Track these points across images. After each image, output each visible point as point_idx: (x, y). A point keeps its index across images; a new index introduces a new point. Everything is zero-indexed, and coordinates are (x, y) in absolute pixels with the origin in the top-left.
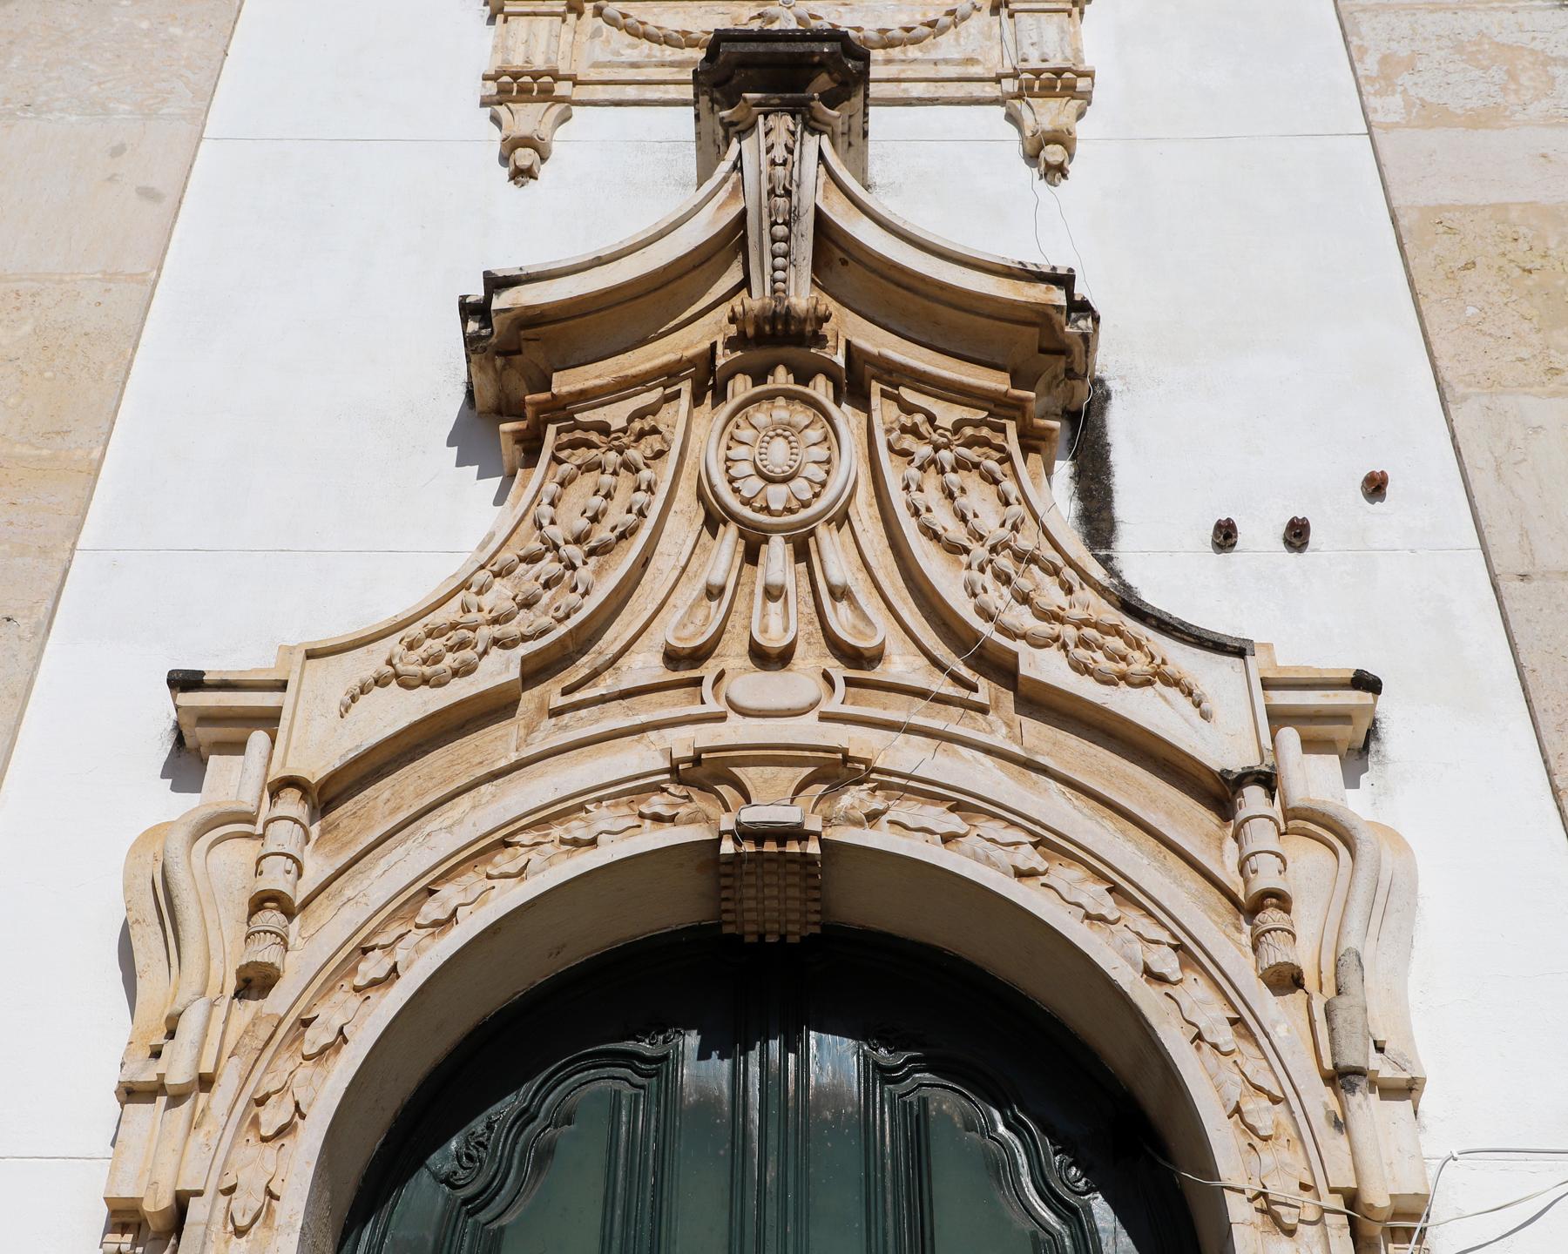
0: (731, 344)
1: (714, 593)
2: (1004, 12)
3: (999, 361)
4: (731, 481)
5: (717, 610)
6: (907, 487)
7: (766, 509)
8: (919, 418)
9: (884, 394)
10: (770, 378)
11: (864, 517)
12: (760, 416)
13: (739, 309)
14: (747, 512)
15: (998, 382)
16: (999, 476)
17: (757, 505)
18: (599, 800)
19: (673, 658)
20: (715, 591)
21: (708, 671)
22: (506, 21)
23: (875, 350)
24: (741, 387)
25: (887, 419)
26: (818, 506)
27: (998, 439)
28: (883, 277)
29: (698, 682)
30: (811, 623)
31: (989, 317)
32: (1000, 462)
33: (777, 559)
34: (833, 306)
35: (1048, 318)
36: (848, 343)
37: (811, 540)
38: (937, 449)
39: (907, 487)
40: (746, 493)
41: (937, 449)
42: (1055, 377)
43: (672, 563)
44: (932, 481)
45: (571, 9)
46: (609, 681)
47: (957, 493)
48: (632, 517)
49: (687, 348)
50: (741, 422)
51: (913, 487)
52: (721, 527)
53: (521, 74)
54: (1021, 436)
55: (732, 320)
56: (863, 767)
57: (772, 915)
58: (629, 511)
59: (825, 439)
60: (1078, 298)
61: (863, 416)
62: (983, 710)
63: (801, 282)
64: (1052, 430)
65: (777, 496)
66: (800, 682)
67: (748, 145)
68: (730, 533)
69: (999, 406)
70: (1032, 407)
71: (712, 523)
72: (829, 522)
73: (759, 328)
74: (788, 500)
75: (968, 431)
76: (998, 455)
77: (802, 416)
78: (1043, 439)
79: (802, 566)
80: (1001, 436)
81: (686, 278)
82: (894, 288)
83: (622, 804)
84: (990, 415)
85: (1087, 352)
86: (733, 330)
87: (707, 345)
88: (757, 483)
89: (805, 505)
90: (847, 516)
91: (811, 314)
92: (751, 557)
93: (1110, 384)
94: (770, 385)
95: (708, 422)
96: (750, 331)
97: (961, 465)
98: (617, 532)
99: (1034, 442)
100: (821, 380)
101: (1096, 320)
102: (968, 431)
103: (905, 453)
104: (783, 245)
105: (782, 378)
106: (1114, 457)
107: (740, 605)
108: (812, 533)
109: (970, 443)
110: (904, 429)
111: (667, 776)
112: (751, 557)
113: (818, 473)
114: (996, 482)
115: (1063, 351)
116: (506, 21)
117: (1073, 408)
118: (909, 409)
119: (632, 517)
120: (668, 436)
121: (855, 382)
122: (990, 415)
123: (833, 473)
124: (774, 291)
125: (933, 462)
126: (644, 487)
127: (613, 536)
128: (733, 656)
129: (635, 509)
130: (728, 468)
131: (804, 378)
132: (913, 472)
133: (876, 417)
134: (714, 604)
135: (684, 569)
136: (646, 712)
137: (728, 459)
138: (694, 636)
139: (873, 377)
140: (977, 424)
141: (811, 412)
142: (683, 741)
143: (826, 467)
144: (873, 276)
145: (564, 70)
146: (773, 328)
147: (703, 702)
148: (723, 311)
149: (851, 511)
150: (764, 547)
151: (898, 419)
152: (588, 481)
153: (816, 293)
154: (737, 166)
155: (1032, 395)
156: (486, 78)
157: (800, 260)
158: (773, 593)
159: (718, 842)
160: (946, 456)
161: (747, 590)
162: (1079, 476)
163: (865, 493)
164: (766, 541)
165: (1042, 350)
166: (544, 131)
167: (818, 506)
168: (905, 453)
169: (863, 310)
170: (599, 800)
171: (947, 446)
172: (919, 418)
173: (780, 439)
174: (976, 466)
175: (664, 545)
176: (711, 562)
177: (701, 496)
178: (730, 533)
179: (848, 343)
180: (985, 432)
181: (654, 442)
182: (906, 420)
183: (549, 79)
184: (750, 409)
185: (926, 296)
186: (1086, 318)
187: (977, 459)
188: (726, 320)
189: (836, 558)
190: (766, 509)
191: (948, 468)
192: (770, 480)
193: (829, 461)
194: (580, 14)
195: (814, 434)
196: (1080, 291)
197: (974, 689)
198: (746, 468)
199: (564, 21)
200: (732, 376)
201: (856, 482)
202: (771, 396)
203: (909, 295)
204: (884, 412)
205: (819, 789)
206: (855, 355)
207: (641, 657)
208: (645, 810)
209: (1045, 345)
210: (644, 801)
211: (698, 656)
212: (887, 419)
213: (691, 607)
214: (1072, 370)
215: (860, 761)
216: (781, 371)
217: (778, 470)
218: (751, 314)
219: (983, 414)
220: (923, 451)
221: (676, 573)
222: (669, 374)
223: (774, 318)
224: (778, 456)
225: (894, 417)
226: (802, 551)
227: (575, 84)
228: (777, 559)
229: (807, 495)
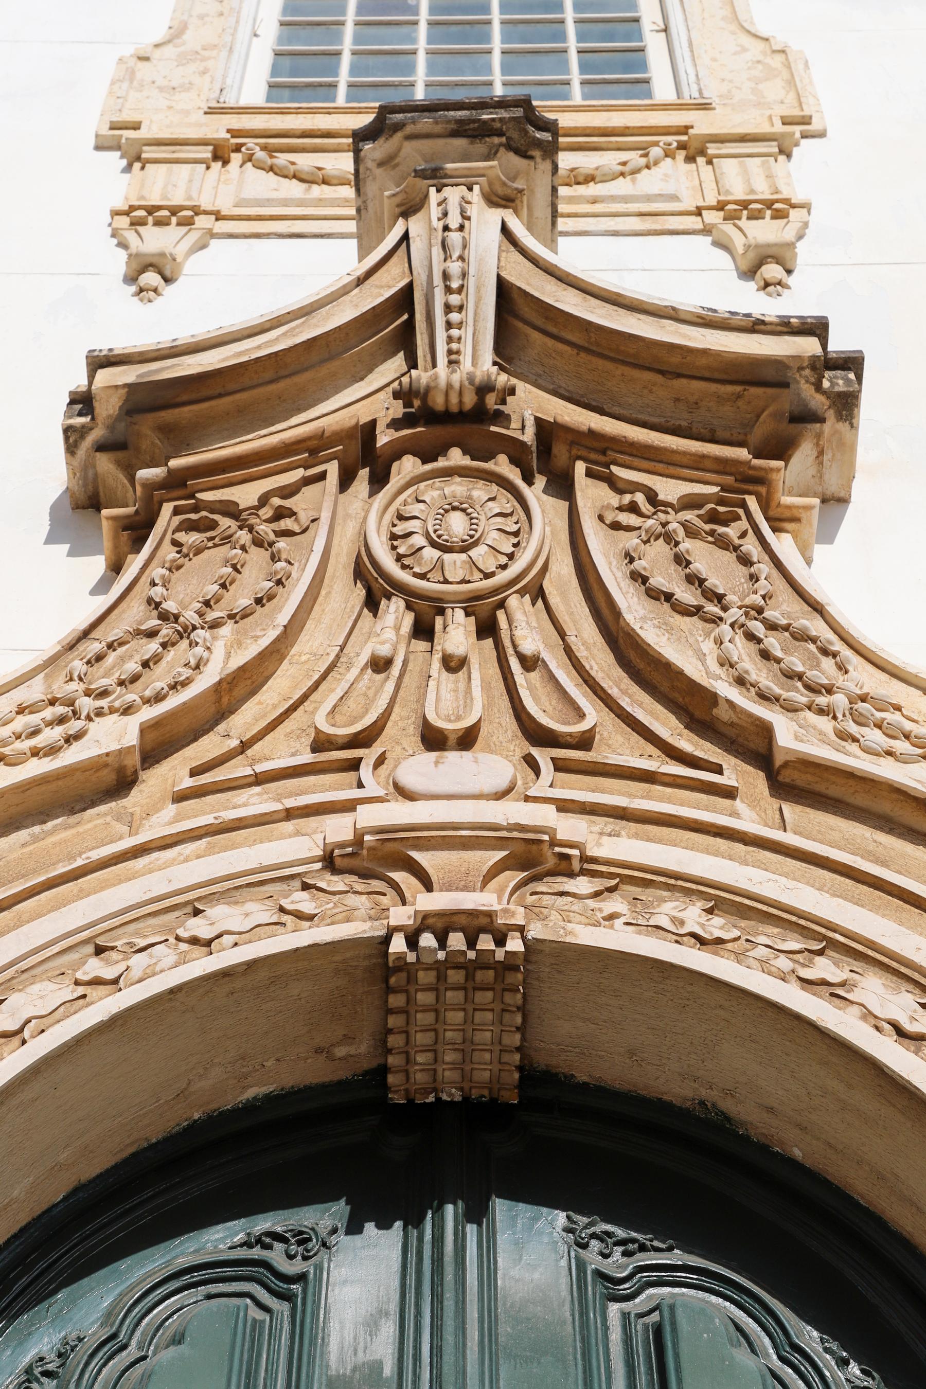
0: (395, 424)
2: (701, 160)
4: (399, 558)
21: (369, 755)
22: (143, 168)
29: (354, 765)
33: (457, 633)
45: (216, 157)
53: (159, 208)
56: (575, 852)
57: (452, 1057)
62: (729, 793)
66: (492, 765)
67: (416, 226)
72: (522, 592)
79: (490, 642)
88: (430, 554)
92: (423, 630)
108: (501, 605)
111: (319, 865)
112: (423, 630)
116: (143, 168)
121: (551, 458)
128: (401, 735)
142: (339, 829)
145: (206, 205)
147: (360, 785)
149: (546, 584)
152: (224, 551)
154: (406, 237)
156: (116, 213)
158: (454, 665)
159: (386, 940)
163: (563, 568)
166: (180, 251)
177: (359, 573)
183: (190, 213)
194: (226, 162)
197: (719, 770)
199: (208, 168)
200: (398, 457)
205: (513, 877)
208: (287, 904)
215: (572, 846)
226: (487, 629)
227: (217, 219)
228: (457, 633)
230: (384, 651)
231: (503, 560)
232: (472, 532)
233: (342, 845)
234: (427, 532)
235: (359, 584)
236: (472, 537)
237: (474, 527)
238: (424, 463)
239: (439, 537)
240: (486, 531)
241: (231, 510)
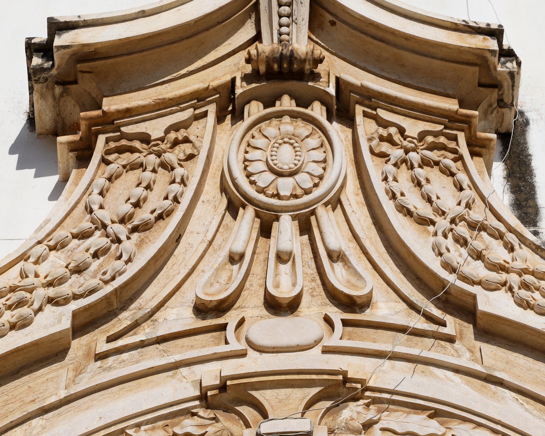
1: (235, 259)
3: (450, 92)
4: (249, 175)
5: (237, 272)
6: (386, 179)
7: (277, 196)
8: (393, 130)
9: (365, 114)
10: (278, 103)
11: (353, 203)
12: (271, 129)
13: (253, 52)
14: (261, 197)
15: (451, 105)
16: (454, 170)
17: (270, 192)
18: (138, 426)
19: (201, 309)
20: (236, 258)
23: (358, 82)
24: (255, 110)
25: (368, 132)
26: (317, 193)
27: (452, 145)
28: (362, 32)
30: (313, 280)
31: (442, 59)
32: (455, 160)
34: (325, 53)
35: (485, 60)
36: (338, 80)
37: (313, 218)
38: (407, 152)
39: (386, 179)
40: (261, 184)
41: (407, 152)
42: (490, 105)
43: (200, 237)
44: (404, 174)
46: (147, 331)
47: (423, 182)
48: (168, 202)
49: (212, 81)
50: (256, 134)
51: (390, 178)
52: (241, 210)
54: (469, 145)
55: (248, 61)
58: (166, 198)
59: (322, 145)
60: (505, 47)
61: (349, 131)
63: (301, 36)
64: (491, 140)
65: (285, 186)
68: (248, 215)
69: (451, 120)
70: (476, 121)
71: (233, 209)
72: (326, 205)
73: (269, 66)
74: (294, 189)
75: (430, 139)
76: (453, 156)
77: (303, 129)
78: (484, 146)
79: (306, 237)
80: (455, 143)
81: (212, 31)
82: (371, 40)
83: (159, 428)
84: (446, 128)
85: (513, 86)
86: (249, 69)
87: (228, 78)
88: (270, 177)
89: (307, 192)
90: (339, 201)
91: (309, 57)
93: (528, 115)
94: (278, 107)
95: (230, 135)
96: (262, 69)
97: (425, 163)
98: (156, 214)
99: (477, 149)
100: (317, 105)
101: (519, 64)
102: (430, 139)
103: (383, 155)
104: (287, 8)
105: (287, 103)
106: (535, 164)
107: (257, 269)
108: (313, 213)
109: (432, 147)
110: (382, 139)
111: (197, 403)
113: (317, 170)
114: (452, 175)
115: (495, 85)
117: (503, 130)
118: (385, 124)
119: (168, 202)
120: (197, 144)
122: (446, 128)
123: (328, 170)
124: (280, 41)
125: (404, 161)
126: (178, 180)
127: (153, 217)
129: (171, 197)
130: (245, 168)
131: (304, 102)
132: (390, 167)
133: (360, 130)
134: (236, 267)
135: (211, 243)
136: (180, 353)
137: (246, 160)
138: (220, 292)
139: (358, 103)
140: (436, 134)
141: (310, 127)
142: (210, 374)
143: (323, 165)
144: (355, 32)
146: (280, 66)
148: (243, 55)
149: (343, 198)
150: (275, 224)
151: (377, 131)
153: (312, 45)
155: (476, 113)
157: (300, 20)
158: (282, 258)
160: (414, 157)
161: (262, 257)
162: (510, 176)
164: (277, 219)
165: (481, 85)
167: (317, 193)
168: (383, 155)
169: (348, 57)
170: (138, 426)
171: (414, 150)
172: (393, 130)
173: (287, 145)
174: (437, 163)
175: (193, 225)
176: (233, 236)
177: (224, 189)
178: (248, 215)
179: (338, 79)
180: (442, 140)
181: (187, 149)
182: (384, 132)
184: (263, 125)
185: (395, 46)
186: (512, 61)
187: (437, 159)
188: (243, 62)
189: (332, 231)
190: (277, 196)
191: (416, 165)
192: (280, 174)
193: (325, 161)
195: (314, 142)
196: (507, 43)
198: (262, 166)
200: (249, 102)
201: (345, 178)
202: (279, 115)
203: (383, 45)
204: (365, 127)
206: (343, 87)
207: (175, 311)
209: (484, 81)
210: (177, 424)
211: (222, 307)
212: (368, 132)
213: (217, 270)
214: (502, 100)
216: (286, 99)
217: (286, 167)
218: (263, 56)
219: (440, 127)
220: (397, 153)
221: (205, 245)
222: (200, 97)
223: (281, 58)
224: (286, 157)
225: (373, 130)
226: (305, 228)
229: (308, 185)
230: (238, 248)
231: (317, 180)
232: (296, 162)
233: (212, 388)
234: (267, 161)
235: (224, 194)
236: (296, 165)
237: (298, 158)
238: (265, 108)
239: (275, 165)
240: (305, 162)
241: (145, 139)
